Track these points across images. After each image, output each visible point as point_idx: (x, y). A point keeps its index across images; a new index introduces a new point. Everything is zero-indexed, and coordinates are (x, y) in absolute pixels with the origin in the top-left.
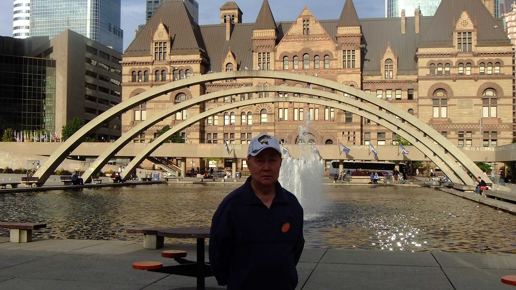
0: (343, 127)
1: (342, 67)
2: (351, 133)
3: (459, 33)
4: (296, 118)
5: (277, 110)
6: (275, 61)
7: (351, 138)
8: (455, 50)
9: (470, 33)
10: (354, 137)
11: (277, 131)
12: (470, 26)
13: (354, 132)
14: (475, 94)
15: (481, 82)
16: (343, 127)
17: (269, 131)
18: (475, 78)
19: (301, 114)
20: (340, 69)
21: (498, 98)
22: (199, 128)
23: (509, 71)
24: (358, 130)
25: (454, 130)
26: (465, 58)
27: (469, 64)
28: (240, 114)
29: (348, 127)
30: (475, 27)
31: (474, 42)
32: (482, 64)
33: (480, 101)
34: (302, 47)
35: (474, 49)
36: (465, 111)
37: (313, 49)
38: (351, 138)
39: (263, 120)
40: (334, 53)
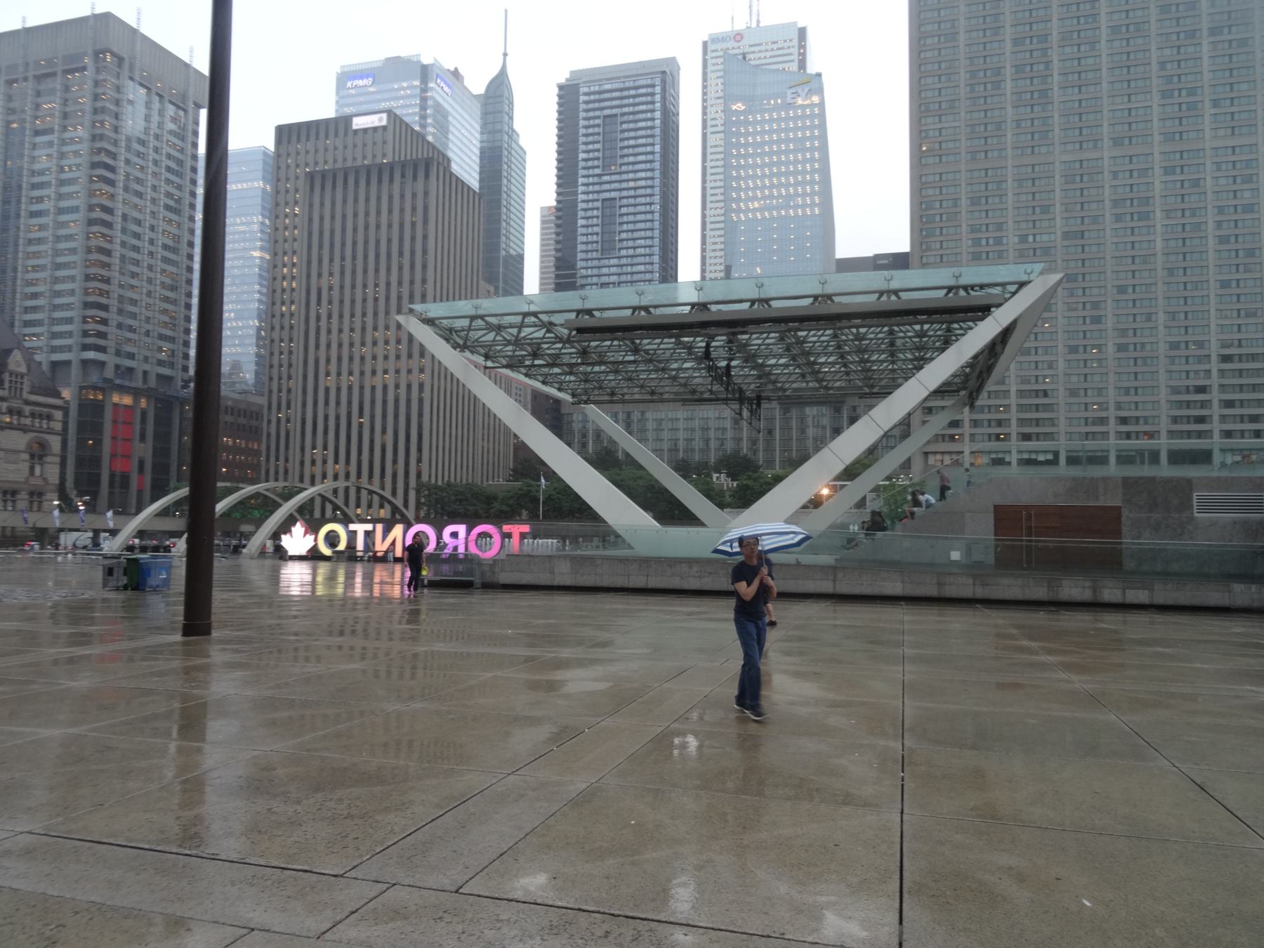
3: (11, 375)
8: (5, 393)
9: (22, 376)
12: (23, 369)
14: (22, 447)
15: (32, 435)
18: (24, 429)
21: (46, 455)
23: (58, 426)
26: (16, 404)
27: (20, 413)
30: (29, 370)
31: (26, 388)
32: (33, 415)
33: (26, 456)
35: (25, 395)
36: (12, 467)
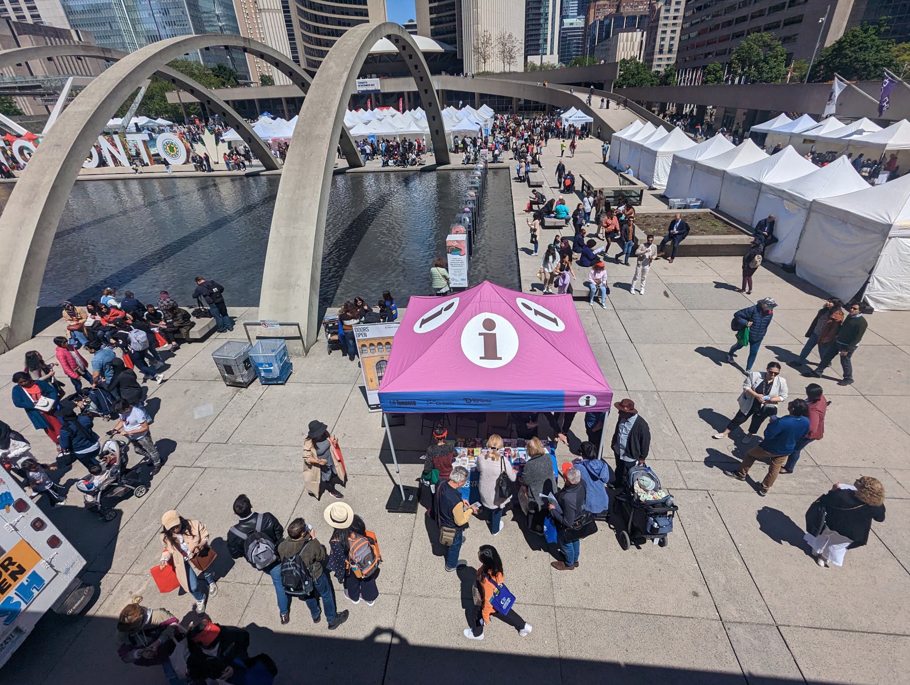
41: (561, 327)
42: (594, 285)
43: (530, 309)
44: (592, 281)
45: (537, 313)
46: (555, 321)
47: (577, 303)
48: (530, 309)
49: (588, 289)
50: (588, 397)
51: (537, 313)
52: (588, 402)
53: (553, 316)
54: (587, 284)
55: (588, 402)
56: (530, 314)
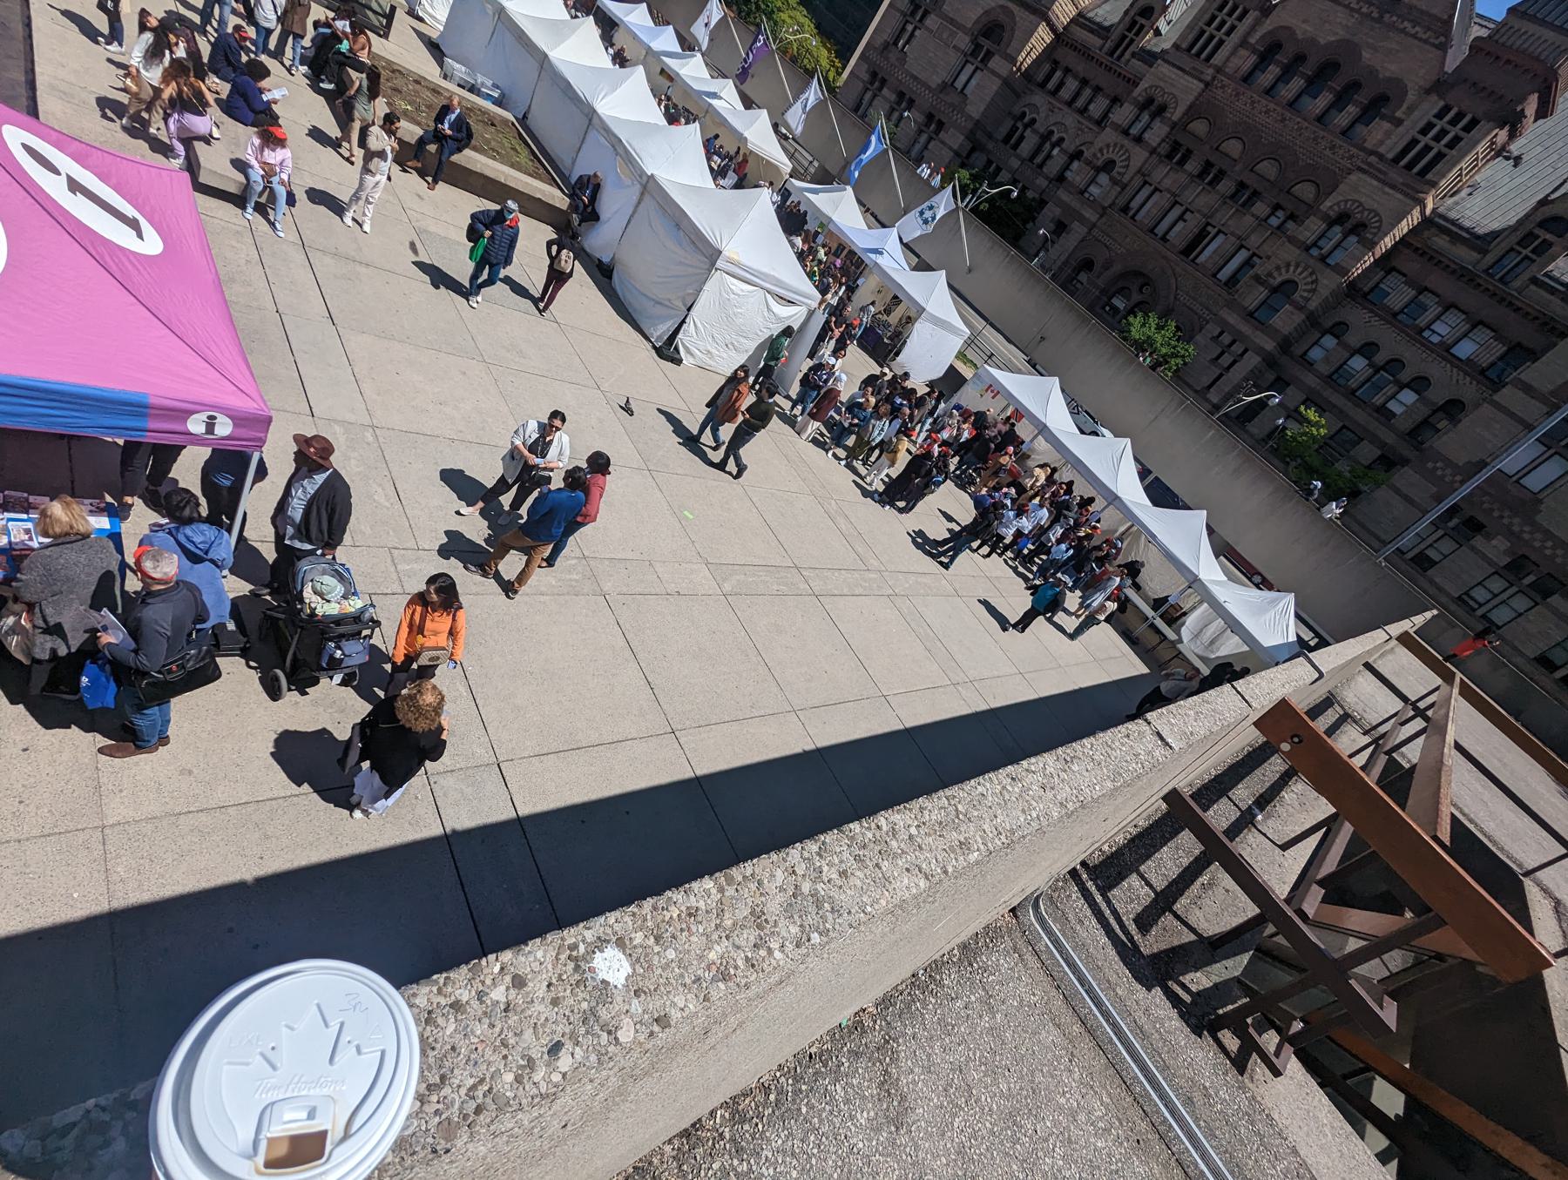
0: (1232, 318)
1: (1390, 156)
2: (1238, 348)
4: (1160, 230)
5: (1138, 181)
6: (1244, 43)
7: (1226, 360)
10: (1235, 362)
11: (1095, 232)
13: (1246, 351)
16: (1232, 318)
17: (1082, 219)
19: (1181, 225)
20: (1381, 157)
22: (970, 125)
24: (1260, 351)
25: (1510, 534)
28: (1071, 149)
29: (1245, 328)
34: (1342, 33)
37: (1366, 55)
38: (1226, 360)
39: (1094, 190)
40: (1411, 97)
41: (152, 244)
42: (257, 173)
43: (56, 172)
44: (254, 162)
45: (74, 186)
46: (133, 224)
47: (203, 201)
48: (56, 172)
49: (241, 178)
50: (212, 418)
51: (74, 186)
52: (210, 427)
53: (130, 211)
54: (241, 165)
55: (210, 427)
56: (55, 187)
